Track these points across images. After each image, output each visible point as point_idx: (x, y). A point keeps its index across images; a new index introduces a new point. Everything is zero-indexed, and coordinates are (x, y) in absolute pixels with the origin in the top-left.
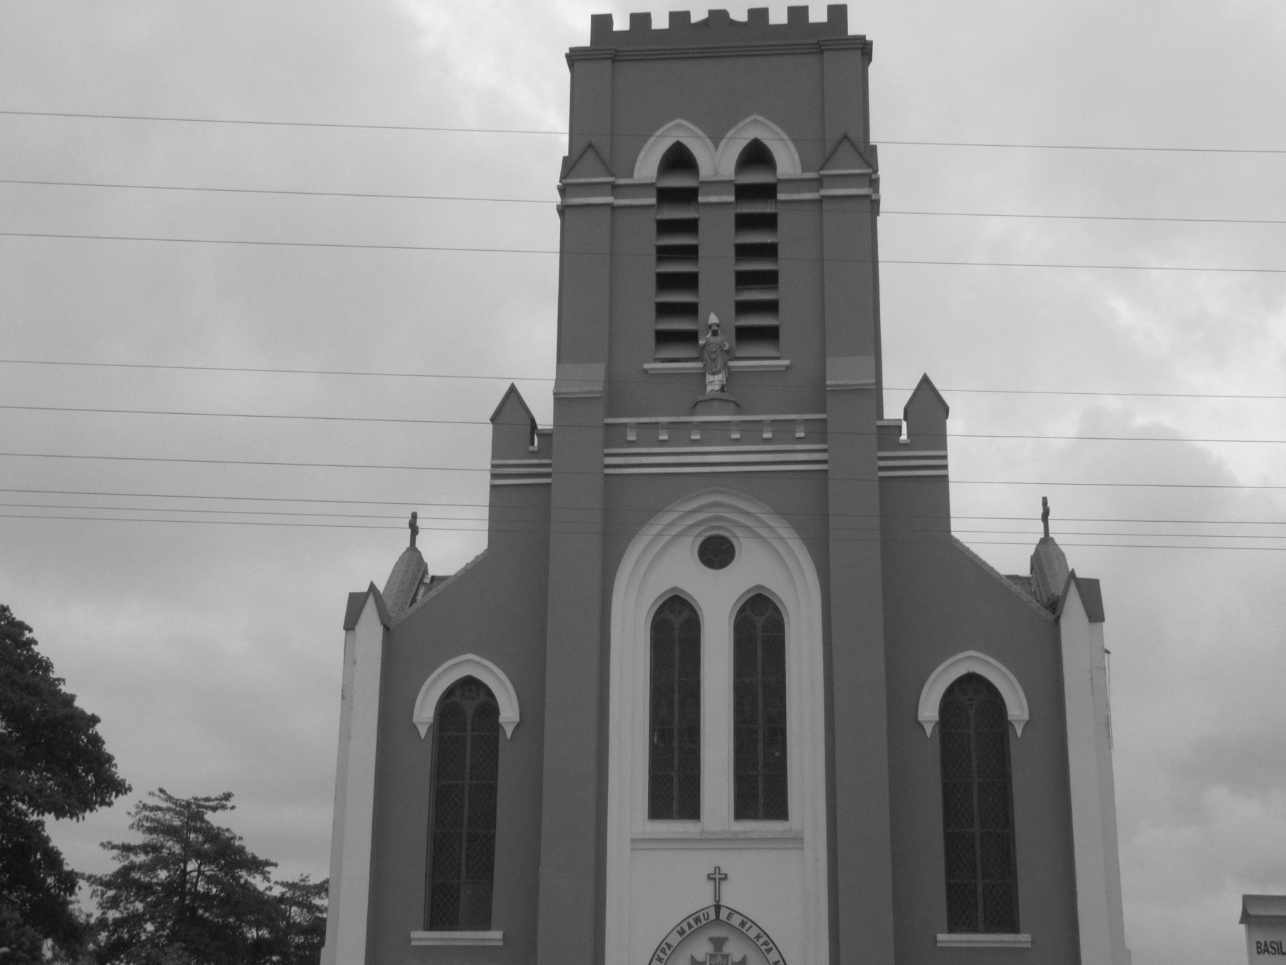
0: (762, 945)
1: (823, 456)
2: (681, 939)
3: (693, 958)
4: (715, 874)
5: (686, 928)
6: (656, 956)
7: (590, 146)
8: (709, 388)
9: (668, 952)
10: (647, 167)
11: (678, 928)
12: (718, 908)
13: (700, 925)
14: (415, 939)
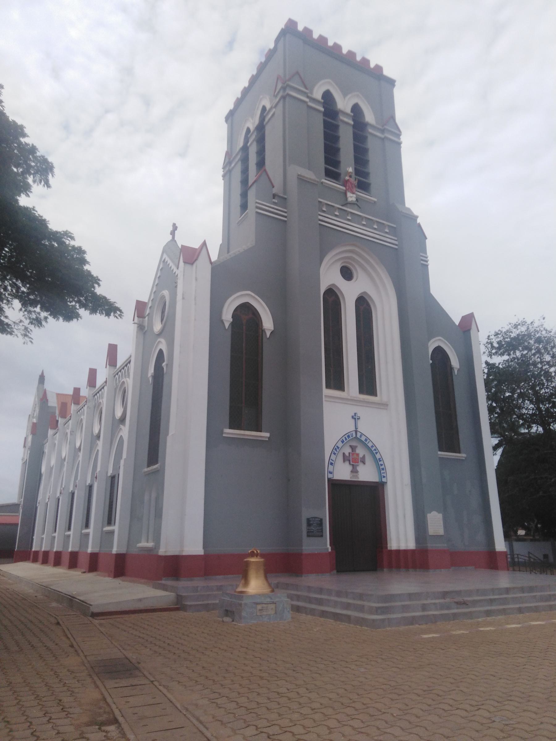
0: (374, 450)
1: (396, 242)
2: (342, 445)
3: (344, 454)
4: (355, 416)
5: (344, 439)
6: (333, 452)
7: (297, 73)
8: (350, 199)
9: (337, 450)
10: (318, 94)
11: (341, 440)
12: (356, 432)
13: (350, 439)
14: (225, 433)
